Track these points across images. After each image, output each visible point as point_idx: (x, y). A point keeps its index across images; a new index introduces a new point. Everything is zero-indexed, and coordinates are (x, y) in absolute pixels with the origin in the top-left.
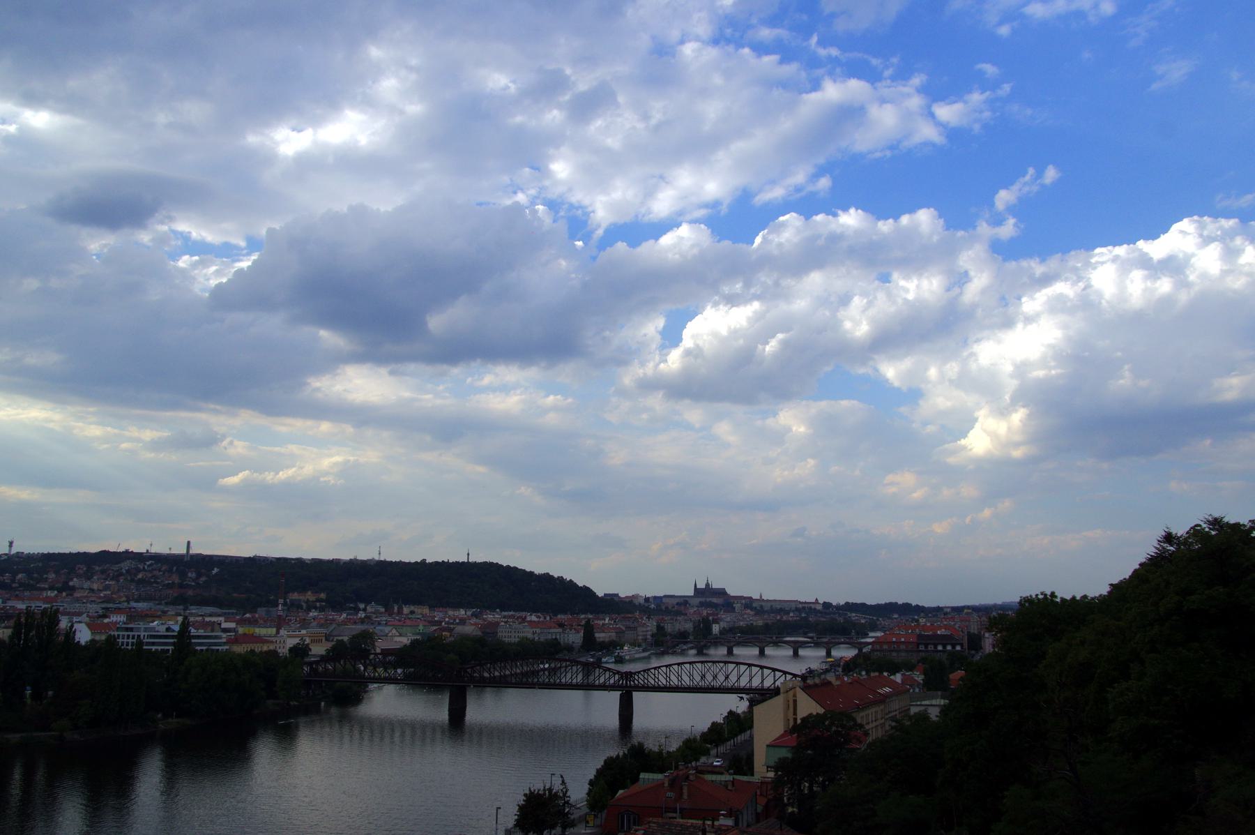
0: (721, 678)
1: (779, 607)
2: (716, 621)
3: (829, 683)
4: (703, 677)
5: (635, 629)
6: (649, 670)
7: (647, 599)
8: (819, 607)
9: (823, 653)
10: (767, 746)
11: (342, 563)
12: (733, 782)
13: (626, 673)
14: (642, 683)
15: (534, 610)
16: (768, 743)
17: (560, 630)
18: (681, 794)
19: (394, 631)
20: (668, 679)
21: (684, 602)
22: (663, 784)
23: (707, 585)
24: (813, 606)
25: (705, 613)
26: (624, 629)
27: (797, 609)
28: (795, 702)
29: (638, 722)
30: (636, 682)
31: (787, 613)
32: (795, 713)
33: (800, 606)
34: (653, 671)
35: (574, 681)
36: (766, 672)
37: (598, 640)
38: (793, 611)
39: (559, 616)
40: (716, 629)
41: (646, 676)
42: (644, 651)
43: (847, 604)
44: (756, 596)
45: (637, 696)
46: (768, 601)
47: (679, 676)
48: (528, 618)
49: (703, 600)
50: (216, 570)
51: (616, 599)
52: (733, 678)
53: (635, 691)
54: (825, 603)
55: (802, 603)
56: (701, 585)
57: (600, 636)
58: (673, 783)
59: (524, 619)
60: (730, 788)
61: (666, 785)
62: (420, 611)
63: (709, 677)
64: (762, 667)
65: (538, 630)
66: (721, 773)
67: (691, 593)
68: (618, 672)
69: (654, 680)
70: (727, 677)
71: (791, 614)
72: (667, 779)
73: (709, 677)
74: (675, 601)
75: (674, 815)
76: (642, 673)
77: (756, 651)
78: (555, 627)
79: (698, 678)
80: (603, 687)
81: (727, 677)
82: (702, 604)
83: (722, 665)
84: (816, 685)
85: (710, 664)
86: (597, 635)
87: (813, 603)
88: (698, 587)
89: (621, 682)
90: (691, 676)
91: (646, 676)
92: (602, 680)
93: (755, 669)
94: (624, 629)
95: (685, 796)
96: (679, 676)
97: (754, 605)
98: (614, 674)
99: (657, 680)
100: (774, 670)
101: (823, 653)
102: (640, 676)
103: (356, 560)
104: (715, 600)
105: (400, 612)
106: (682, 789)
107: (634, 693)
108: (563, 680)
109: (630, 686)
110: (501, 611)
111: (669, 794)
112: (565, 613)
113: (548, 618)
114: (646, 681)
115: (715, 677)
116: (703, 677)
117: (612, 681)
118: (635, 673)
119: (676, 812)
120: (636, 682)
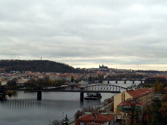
0: (106, 89)
1: (121, 71)
2: (105, 75)
3: (133, 90)
4: (101, 89)
5: (84, 77)
6: (88, 87)
7: (87, 69)
8: (131, 71)
9: (132, 82)
11: (9, 61)
12: (108, 114)
13: (82, 88)
15: (58, 72)
16: (117, 104)
18: (95, 118)
19: (23, 78)
21: (96, 70)
22: (91, 115)
23: (103, 65)
24: (130, 71)
25: (102, 72)
27: (126, 72)
28: (124, 95)
31: (123, 72)
32: (124, 98)
33: (126, 71)
34: (89, 87)
35: (69, 90)
36: (117, 87)
37: (74, 79)
38: (125, 72)
40: (105, 77)
42: (86, 82)
43: (138, 70)
44: (115, 68)
45: (84, 93)
46: (118, 70)
47: (95, 88)
48: (57, 74)
49: (101, 69)
51: (79, 69)
52: (109, 89)
53: (84, 92)
54: (133, 70)
55: (127, 70)
56: (101, 66)
57: (75, 79)
58: (93, 115)
59: (56, 74)
60: (108, 116)
61: (92, 115)
62: (29, 73)
63: (103, 89)
64: (116, 86)
65: (60, 77)
66: (106, 112)
67: (99, 68)
70: (107, 89)
71: (124, 73)
72: (92, 114)
73: (103, 89)
74: (95, 69)
75: (94, 122)
77: (115, 82)
79: (100, 89)
80: (76, 91)
81: (107, 89)
82: (101, 71)
83: (106, 86)
84: (130, 90)
85: (103, 85)
86: (74, 78)
87: (129, 70)
88: (100, 66)
90: (98, 88)
92: (76, 90)
93: (114, 87)
95: (96, 118)
96: (95, 88)
97: (115, 70)
100: (119, 87)
101: (132, 82)
103: (12, 60)
104: (105, 69)
105: (24, 73)
106: (95, 116)
107: (84, 93)
108: (66, 90)
109: (83, 91)
110: (50, 72)
111: (92, 117)
113: (62, 74)
115: (104, 89)
116: (101, 89)
117: (78, 90)
118: (84, 88)
119: (94, 122)
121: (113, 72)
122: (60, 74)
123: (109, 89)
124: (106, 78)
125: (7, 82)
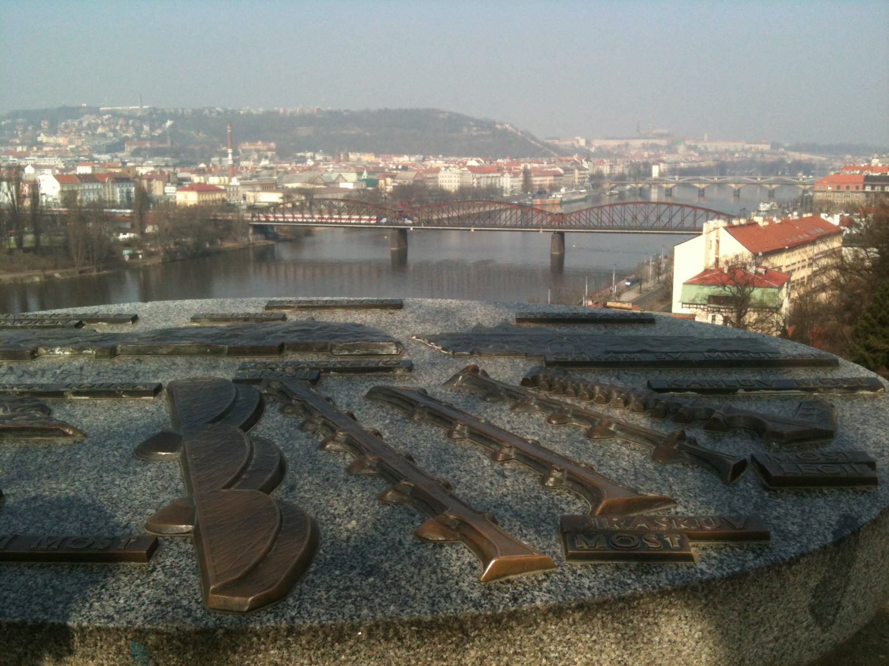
2: (657, 163)
3: (756, 223)
4: (635, 218)
10: (684, 284)
14: (574, 224)
16: (685, 280)
17: (499, 175)
20: (599, 220)
25: (646, 154)
26: (562, 171)
28: (718, 242)
29: (570, 262)
30: (568, 223)
31: (732, 154)
32: (717, 253)
39: (499, 161)
40: (655, 171)
41: (578, 217)
50: (169, 123)
59: (465, 164)
65: (478, 175)
68: (551, 214)
69: (586, 221)
70: (659, 218)
71: (737, 155)
76: (574, 214)
78: (494, 172)
79: (629, 218)
81: (659, 218)
82: (644, 147)
84: (741, 225)
85: (641, 205)
89: (553, 224)
91: (578, 217)
94: (562, 171)
98: (547, 216)
99: (588, 221)
102: (573, 218)
104: (657, 142)
105: (347, 159)
108: (498, 222)
112: (504, 157)
114: (578, 223)
117: (544, 223)
120: (568, 223)
121: (692, 152)
122: (478, 162)
123: (665, 220)
124: (661, 174)
125: (281, 195)
